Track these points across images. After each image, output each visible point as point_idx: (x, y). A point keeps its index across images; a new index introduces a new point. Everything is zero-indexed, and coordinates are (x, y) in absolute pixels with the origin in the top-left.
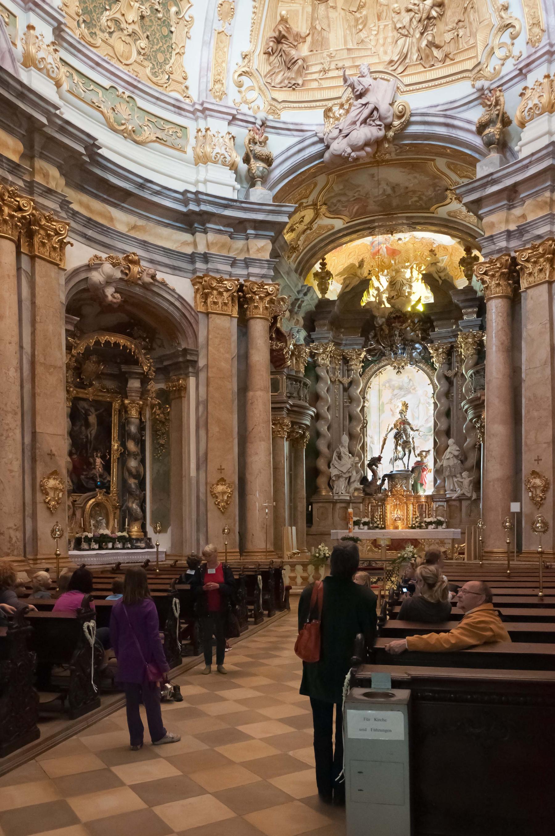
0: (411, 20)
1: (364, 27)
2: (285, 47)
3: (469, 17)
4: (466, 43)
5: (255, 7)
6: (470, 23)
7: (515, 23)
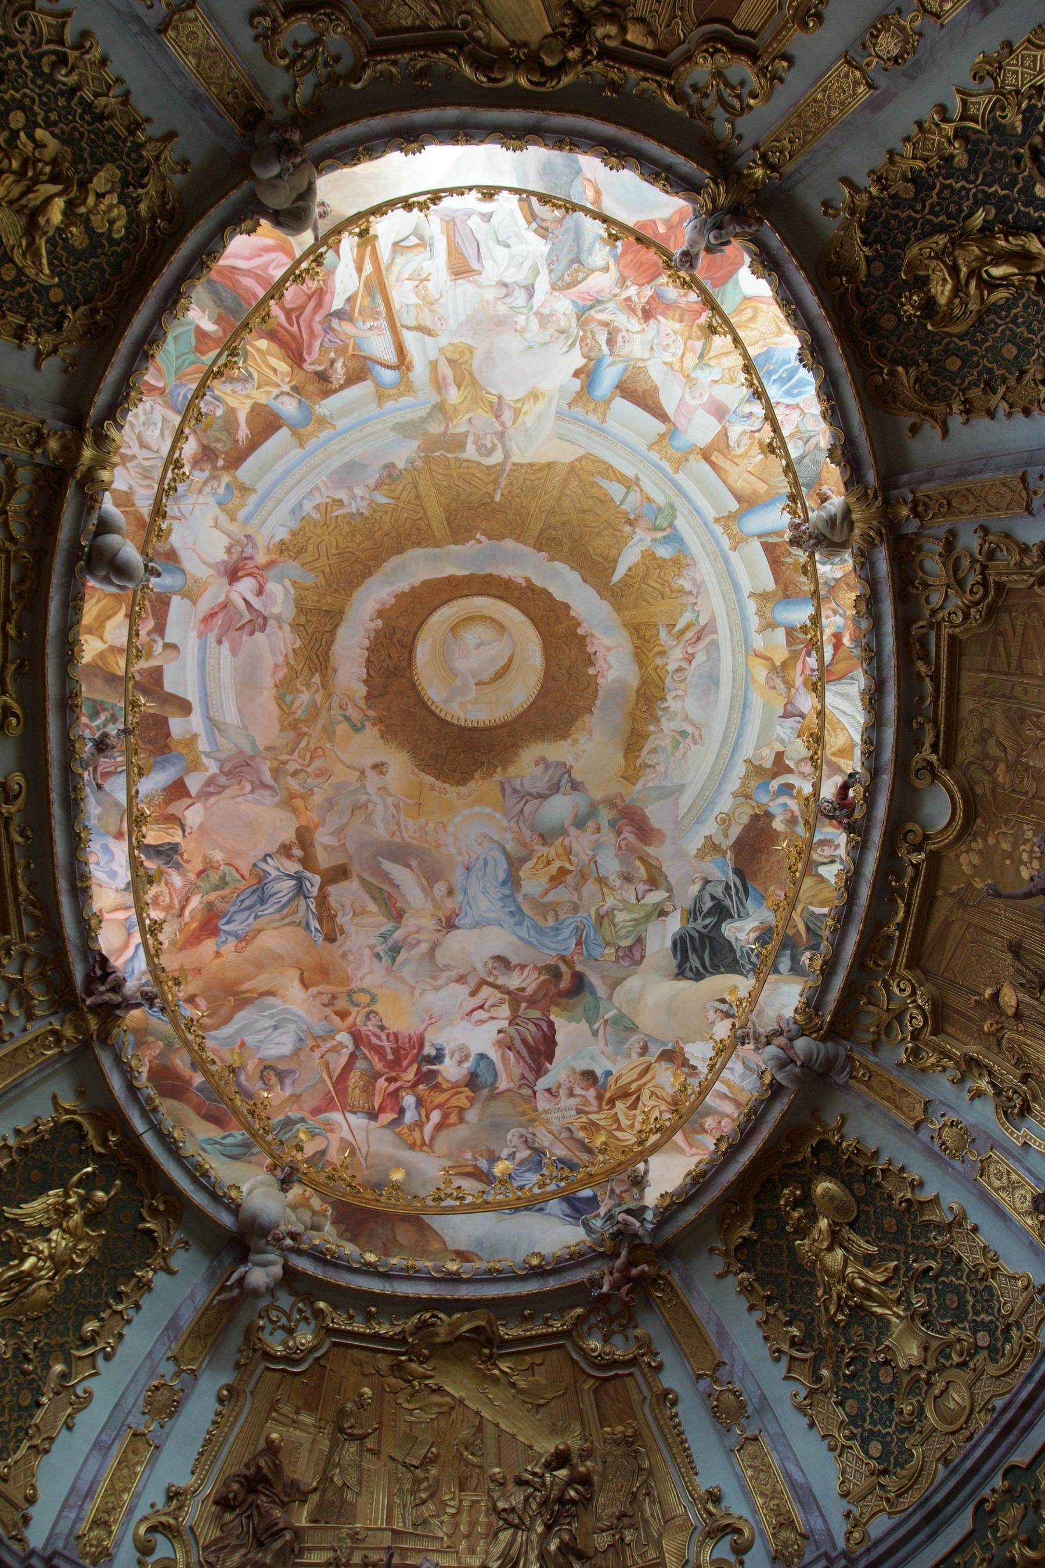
0: (526, 1500)
1: (431, 1496)
2: (262, 1500)
3: (641, 1510)
4: (640, 1556)
5: (217, 1414)
6: (646, 1521)
7: (739, 1524)
